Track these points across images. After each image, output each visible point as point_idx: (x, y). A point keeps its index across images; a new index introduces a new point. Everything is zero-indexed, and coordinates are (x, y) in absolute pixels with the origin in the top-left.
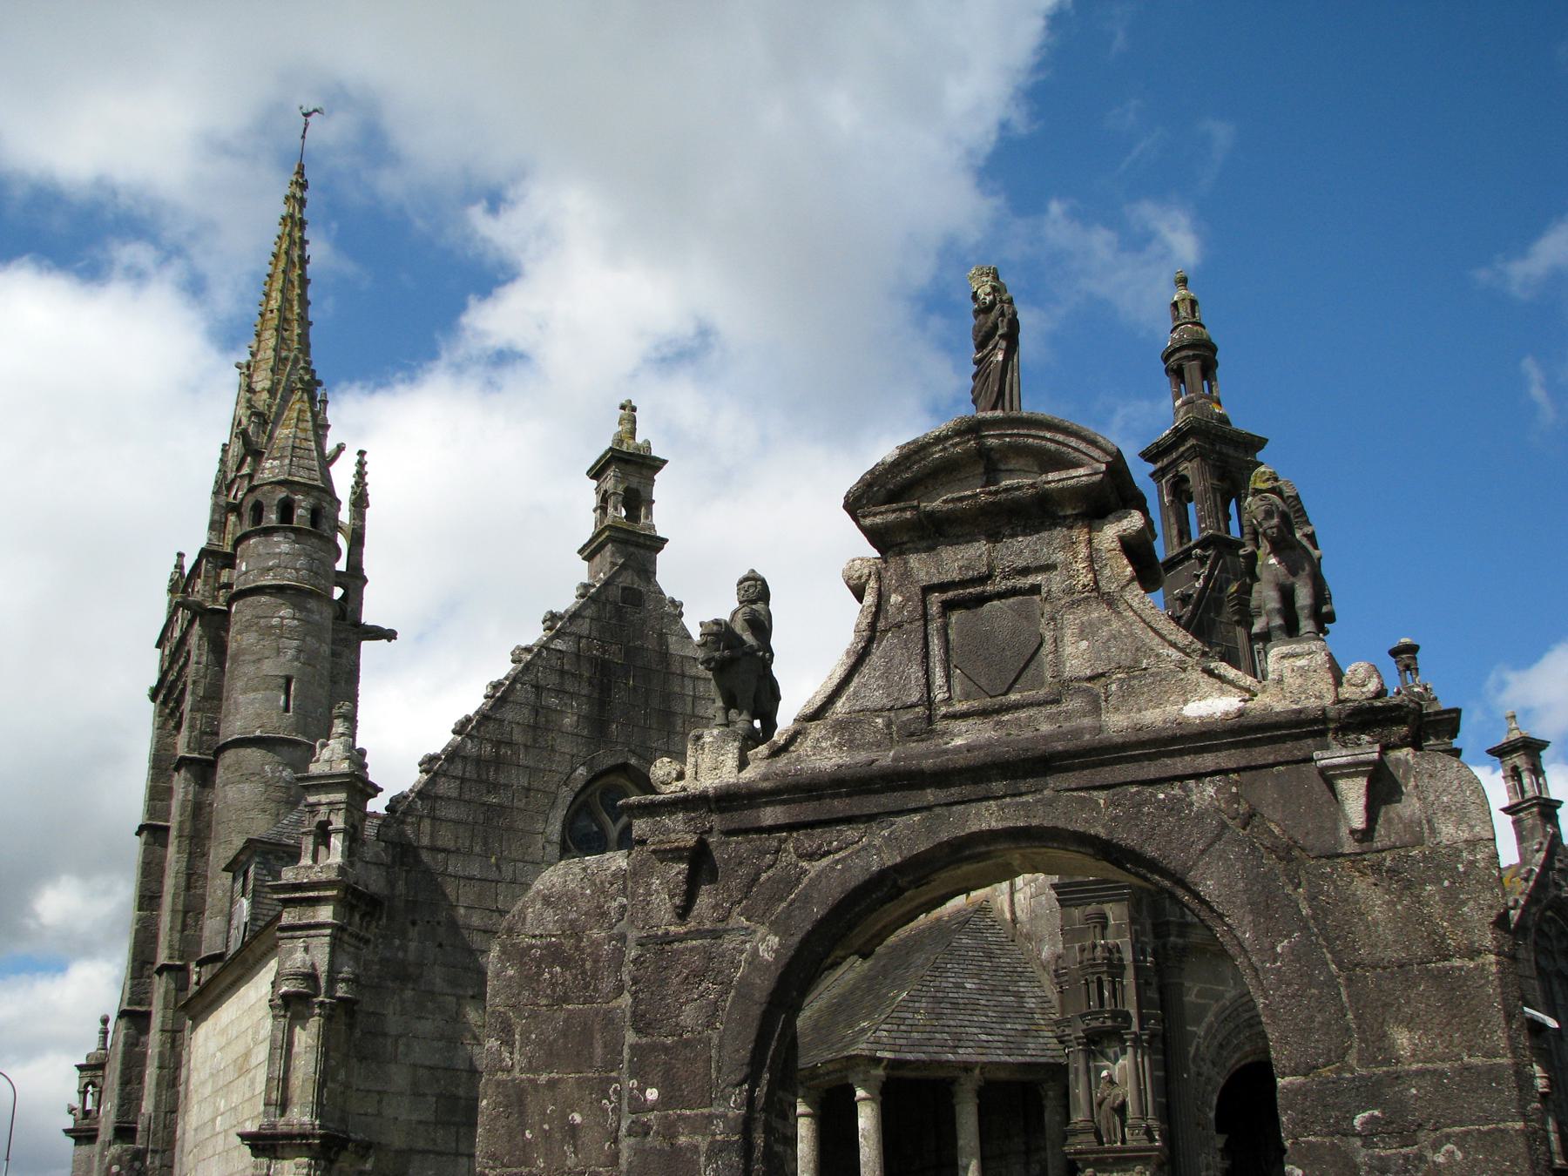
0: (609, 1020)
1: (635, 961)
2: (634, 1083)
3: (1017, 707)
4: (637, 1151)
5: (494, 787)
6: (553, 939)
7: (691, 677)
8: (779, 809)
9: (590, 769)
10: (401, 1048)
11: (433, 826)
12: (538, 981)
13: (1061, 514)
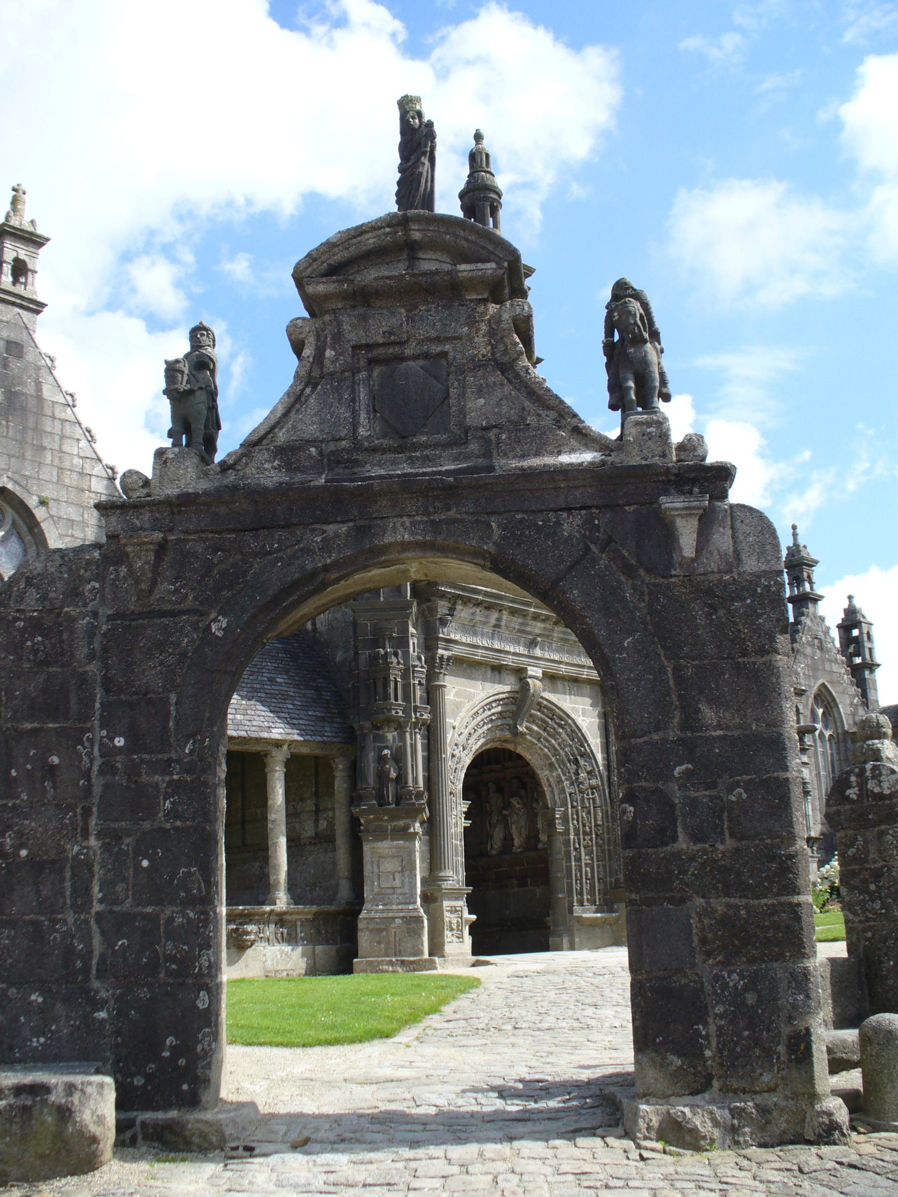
0: (83, 680)
1: (104, 635)
2: (104, 733)
3: (425, 446)
4: (106, 787)
6: (35, 614)
7: (60, 419)
12: (22, 648)
13: (468, 297)
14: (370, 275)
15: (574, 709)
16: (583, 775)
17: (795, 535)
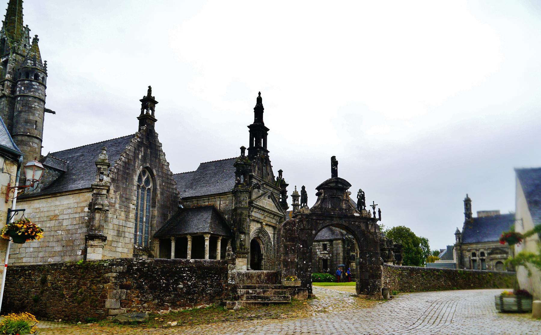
5: (128, 169)
9: (143, 167)
10: (112, 220)
11: (118, 175)
14: (331, 185)
16: (269, 247)
17: (296, 188)
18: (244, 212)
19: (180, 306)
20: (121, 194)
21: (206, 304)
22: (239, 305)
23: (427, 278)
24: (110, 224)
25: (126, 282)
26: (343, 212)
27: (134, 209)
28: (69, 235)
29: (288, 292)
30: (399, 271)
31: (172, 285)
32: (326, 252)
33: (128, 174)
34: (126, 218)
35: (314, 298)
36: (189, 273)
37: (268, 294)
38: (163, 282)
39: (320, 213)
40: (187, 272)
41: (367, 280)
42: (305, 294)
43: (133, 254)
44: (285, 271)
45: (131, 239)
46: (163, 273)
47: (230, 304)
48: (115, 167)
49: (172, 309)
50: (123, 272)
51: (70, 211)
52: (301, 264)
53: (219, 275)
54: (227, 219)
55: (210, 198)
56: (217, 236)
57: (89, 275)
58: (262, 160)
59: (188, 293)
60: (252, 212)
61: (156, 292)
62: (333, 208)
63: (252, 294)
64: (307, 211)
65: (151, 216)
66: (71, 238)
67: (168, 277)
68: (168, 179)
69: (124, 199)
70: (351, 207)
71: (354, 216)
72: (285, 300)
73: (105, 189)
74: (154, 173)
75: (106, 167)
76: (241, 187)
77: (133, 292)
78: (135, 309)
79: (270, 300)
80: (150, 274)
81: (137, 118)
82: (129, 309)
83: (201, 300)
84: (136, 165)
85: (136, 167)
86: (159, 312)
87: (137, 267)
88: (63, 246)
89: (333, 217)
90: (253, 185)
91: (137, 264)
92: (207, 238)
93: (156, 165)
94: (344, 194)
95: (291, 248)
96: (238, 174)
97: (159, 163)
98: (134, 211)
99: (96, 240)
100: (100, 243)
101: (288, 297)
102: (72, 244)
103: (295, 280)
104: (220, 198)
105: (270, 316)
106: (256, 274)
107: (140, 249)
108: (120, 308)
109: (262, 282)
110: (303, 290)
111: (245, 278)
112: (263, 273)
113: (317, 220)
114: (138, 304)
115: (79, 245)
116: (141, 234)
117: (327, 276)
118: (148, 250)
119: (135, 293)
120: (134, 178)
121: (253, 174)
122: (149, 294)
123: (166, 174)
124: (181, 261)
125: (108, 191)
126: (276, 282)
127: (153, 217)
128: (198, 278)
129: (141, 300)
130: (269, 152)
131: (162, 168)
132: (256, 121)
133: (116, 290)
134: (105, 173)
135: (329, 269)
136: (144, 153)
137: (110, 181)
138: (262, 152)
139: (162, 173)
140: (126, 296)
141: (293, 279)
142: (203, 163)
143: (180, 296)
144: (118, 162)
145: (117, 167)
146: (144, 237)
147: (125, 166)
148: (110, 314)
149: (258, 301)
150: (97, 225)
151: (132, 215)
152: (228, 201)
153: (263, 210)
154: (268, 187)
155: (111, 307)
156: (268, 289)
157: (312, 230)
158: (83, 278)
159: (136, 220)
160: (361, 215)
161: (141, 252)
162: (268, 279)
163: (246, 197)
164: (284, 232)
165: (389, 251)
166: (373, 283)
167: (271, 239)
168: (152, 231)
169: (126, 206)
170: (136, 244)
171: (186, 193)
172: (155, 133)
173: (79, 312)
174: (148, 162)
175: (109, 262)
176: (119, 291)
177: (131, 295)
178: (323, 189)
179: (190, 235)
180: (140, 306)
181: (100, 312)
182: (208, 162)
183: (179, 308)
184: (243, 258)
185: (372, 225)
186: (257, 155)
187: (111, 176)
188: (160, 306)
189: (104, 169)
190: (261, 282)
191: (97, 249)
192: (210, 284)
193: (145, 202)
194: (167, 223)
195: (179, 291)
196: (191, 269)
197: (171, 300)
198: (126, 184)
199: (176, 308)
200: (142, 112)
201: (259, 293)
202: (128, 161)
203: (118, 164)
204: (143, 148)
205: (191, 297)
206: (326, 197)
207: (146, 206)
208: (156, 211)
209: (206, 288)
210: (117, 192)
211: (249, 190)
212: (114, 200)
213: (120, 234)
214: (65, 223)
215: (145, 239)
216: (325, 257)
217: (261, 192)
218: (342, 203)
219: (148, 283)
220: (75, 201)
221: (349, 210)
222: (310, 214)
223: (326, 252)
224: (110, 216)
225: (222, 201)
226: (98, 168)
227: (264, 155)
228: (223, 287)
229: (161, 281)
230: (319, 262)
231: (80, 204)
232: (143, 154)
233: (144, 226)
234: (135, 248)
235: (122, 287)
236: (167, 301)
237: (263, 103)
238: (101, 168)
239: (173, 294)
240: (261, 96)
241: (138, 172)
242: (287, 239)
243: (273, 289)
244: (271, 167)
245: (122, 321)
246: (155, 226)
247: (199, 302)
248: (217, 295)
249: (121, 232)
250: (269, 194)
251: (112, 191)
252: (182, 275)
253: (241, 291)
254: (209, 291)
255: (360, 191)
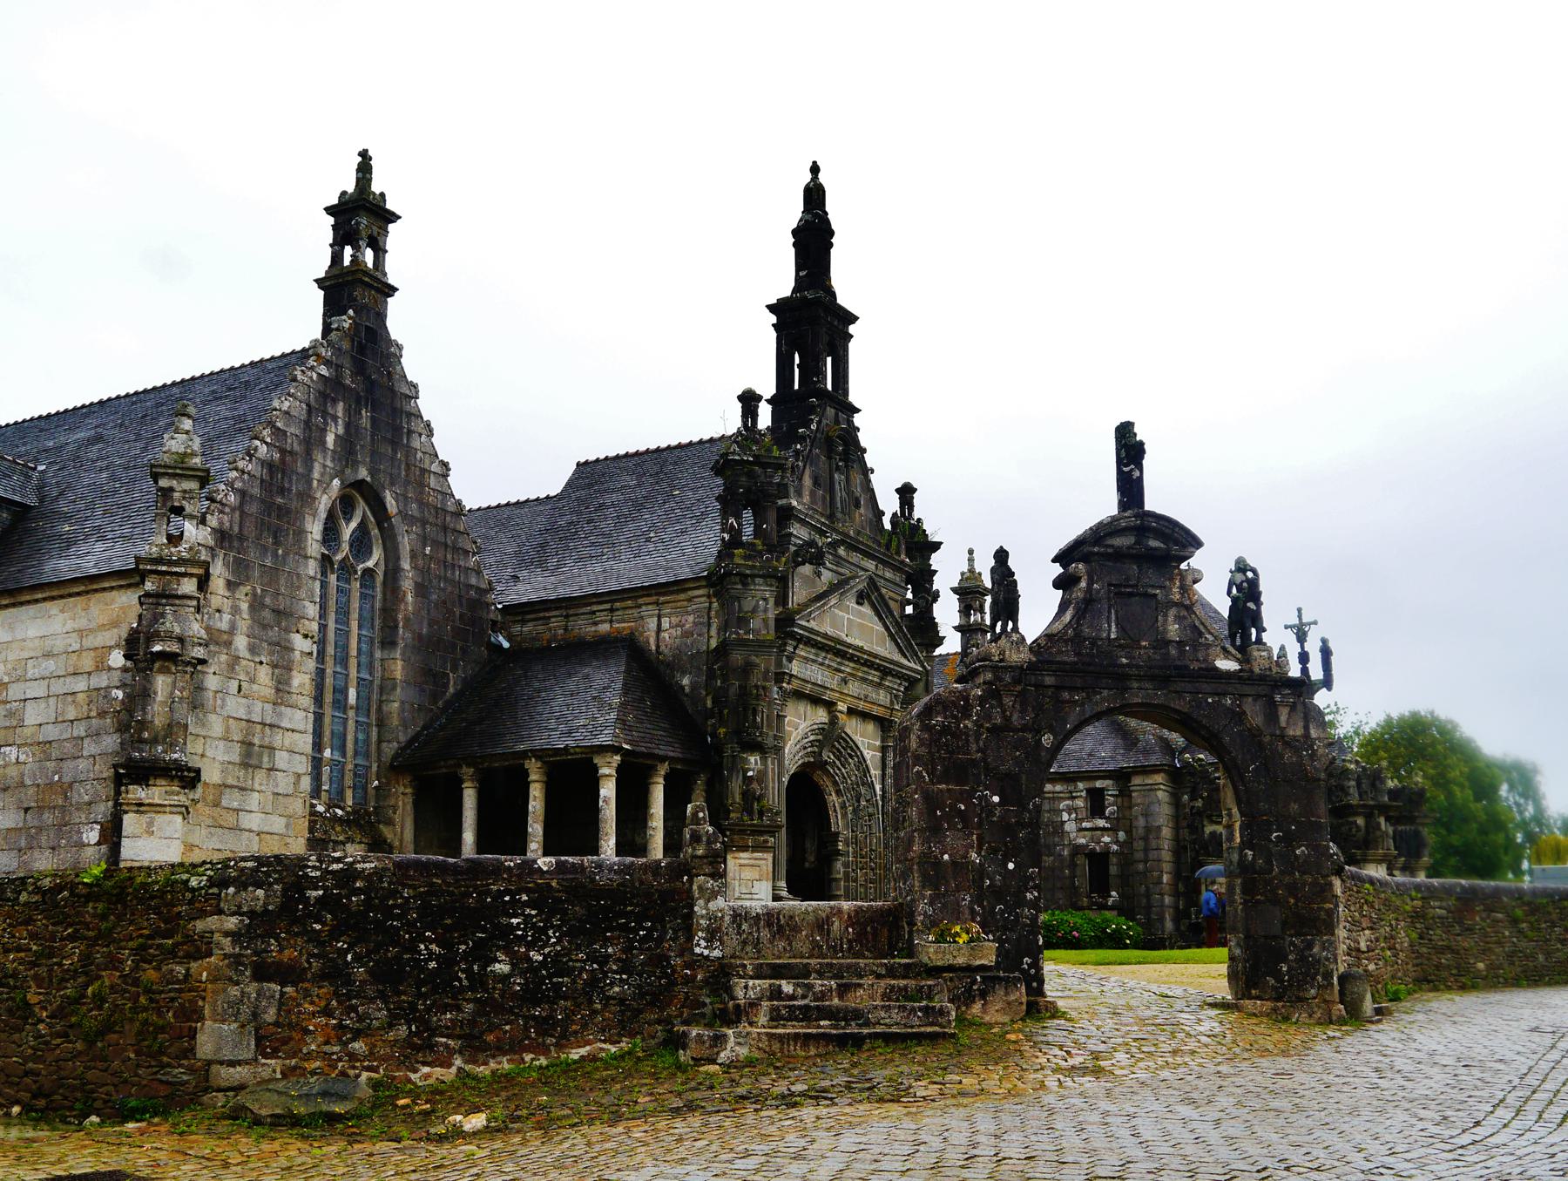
5: (282, 491)
7: (406, 412)
8: (1053, 679)
9: (342, 483)
11: (240, 516)
14: (1118, 541)
15: (863, 742)
17: (971, 560)
18: (757, 661)
19: (499, 1050)
20: (255, 595)
21: (604, 1042)
22: (739, 1044)
23: (1532, 928)
24: (212, 717)
25: (280, 951)
26: (1168, 653)
27: (310, 654)
28: (51, 765)
29: (941, 991)
30: (1412, 900)
31: (467, 962)
32: (1101, 823)
33: (283, 512)
34: (278, 690)
35: (1053, 1017)
36: (533, 912)
37: (859, 999)
38: (431, 953)
39: (1073, 659)
40: (528, 911)
41: (1275, 937)
42: (1012, 998)
43: (308, 840)
44: (931, 904)
45: (299, 776)
46: (430, 916)
47: (704, 1042)
48: (230, 484)
49: (466, 1062)
50: (266, 910)
51: (50, 666)
52: (995, 873)
53: (659, 920)
54: (687, 689)
55: (618, 605)
56: (649, 762)
57: (131, 922)
58: (829, 445)
59: (532, 996)
60: (790, 660)
61: (399, 993)
62: (1129, 640)
63: (792, 997)
64: (1019, 652)
65: (377, 682)
66: (56, 778)
67: (448, 929)
68: (445, 528)
69: (267, 614)
70: (1201, 634)
71: (1216, 669)
72: (932, 1024)
73: (191, 575)
74: (388, 506)
75: (193, 485)
76: (746, 557)
77: (307, 994)
78: (318, 1063)
79: (867, 1024)
80: (376, 921)
81: (316, 281)
82: (293, 1062)
83: (585, 1026)
84: (316, 475)
85: (315, 483)
86: (413, 1076)
87: (321, 892)
88: (26, 810)
89: (1128, 677)
90: (793, 548)
91: (322, 878)
92: (608, 769)
93: (395, 471)
94: (1172, 579)
95: (953, 807)
96: (730, 504)
97: (408, 465)
98: (311, 664)
99: (158, 782)
100: (173, 793)
101: (941, 1008)
102: (60, 802)
103: (971, 940)
104: (657, 603)
105: (870, 1089)
106: (811, 917)
107: (335, 818)
108: (256, 1060)
109: (835, 950)
110: (1007, 980)
111: (765, 934)
112: (840, 911)
113: (1059, 688)
114: (327, 1043)
115: (90, 804)
116: (337, 757)
117: (1107, 922)
118: (369, 822)
119: (315, 999)
120: (308, 527)
121: (795, 503)
122: (372, 1000)
123: (436, 508)
124: (502, 863)
125: (203, 582)
126: (892, 947)
127: (387, 686)
128: (572, 933)
129: (340, 1026)
130: (858, 411)
131: (422, 485)
132: (800, 284)
133: (237, 983)
134: (189, 508)
135: (1114, 893)
136: (347, 426)
137: (211, 543)
138: (830, 412)
139: (422, 504)
140: (279, 1010)
141: (965, 937)
142: (587, 463)
143: (499, 1008)
144: (241, 464)
145: (238, 485)
146: (350, 767)
147: (271, 478)
148: (214, 1082)
149: (819, 1027)
150: (159, 722)
151: (301, 680)
152: (691, 618)
153: (841, 654)
154: (855, 557)
155: (220, 1057)
156: (861, 977)
157: (1038, 732)
158: (105, 937)
159: (318, 699)
160: (1246, 667)
161: (338, 829)
162: (860, 936)
163: (765, 599)
164: (921, 742)
165: (1369, 817)
166: (1302, 951)
167: (873, 772)
168: (384, 745)
169: (278, 644)
170: (319, 798)
171: (521, 587)
172: (390, 342)
173: (90, 1075)
174: (364, 463)
175: (209, 872)
176: (252, 989)
177: (299, 1005)
178: (1085, 559)
179: (538, 758)
180: (337, 1049)
181: (175, 1076)
182: (607, 458)
183: (494, 1057)
184: (756, 848)
185: (1293, 708)
186: (807, 425)
187: (213, 521)
188: (418, 1049)
189: (185, 491)
190: (829, 947)
191: (160, 819)
192: (619, 960)
193: (354, 625)
194: (444, 710)
195: (494, 988)
196: (543, 898)
197: (461, 1027)
198: (277, 555)
199: (481, 1057)
200: (337, 258)
201: (822, 996)
202: (282, 460)
203: (243, 472)
204: (340, 406)
205: (544, 1014)
206: (1098, 591)
207: (359, 642)
208: (400, 663)
209: (605, 974)
210: (240, 584)
211: (776, 569)
212: (226, 617)
213: (252, 756)
214: (32, 715)
215: (355, 775)
216: (1099, 842)
217: (827, 576)
218: (1166, 616)
219: (369, 953)
220: (70, 625)
221: (1196, 646)
222: (1032, 667)
223: (1101, 823)
224: (212, 682)
225: (665, 616)
226: (161, 489)
227: (837, 422)
228: (674, 971)
229: (422, 947)
230: (1073, 865)
231: (90, 638)
232: (341, 431)
233: (351, 725)
234: (313, 813)
235: (262, 973)
236: (447, 1028)
237: (832, 207)
238: (171, 489)
239: (468, 1001)
240: (822, 178)
241: (324, 503)
242: (934, 769)
243: (879, 976)
244: (866, 472)
245: (264, 1112)
246: (395, 722)
247: (576, 1032)
248: (648, 1004)
249: (256, 748)
250: (861, 587)
251: (218, 583)
252: (504, 920)
253: (747, 988)
254: (617, 989)
255: (1241, 567)
